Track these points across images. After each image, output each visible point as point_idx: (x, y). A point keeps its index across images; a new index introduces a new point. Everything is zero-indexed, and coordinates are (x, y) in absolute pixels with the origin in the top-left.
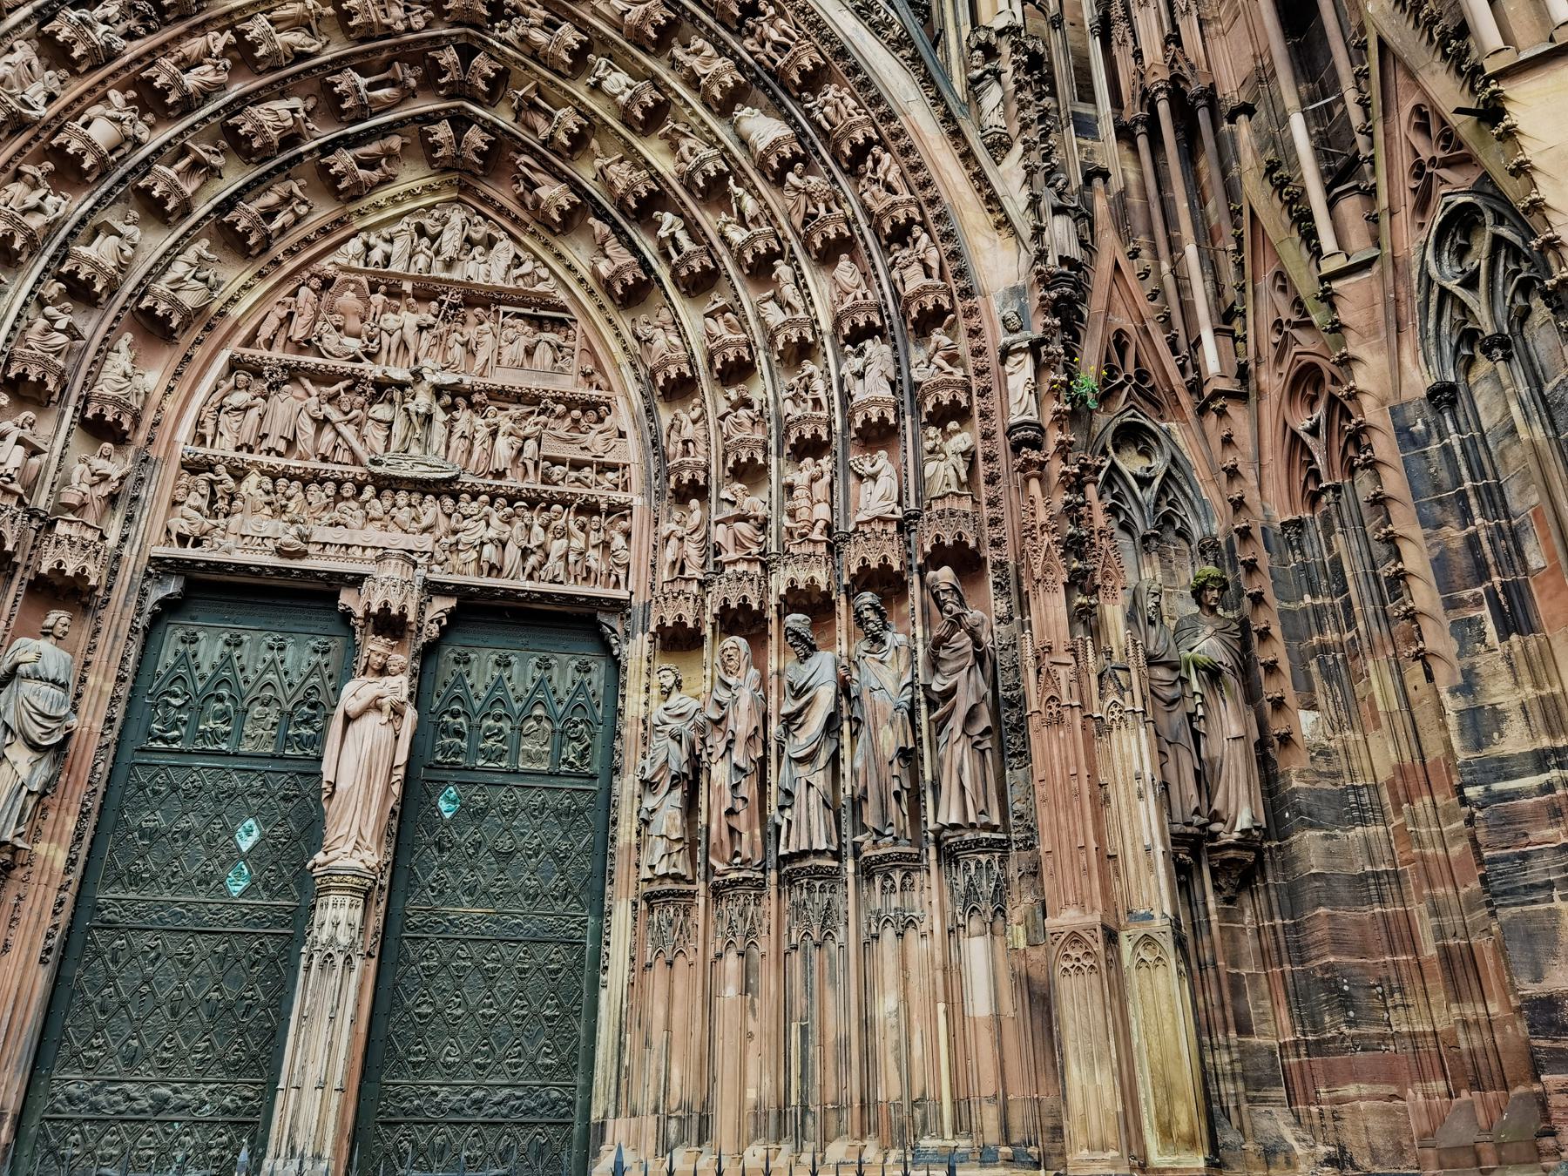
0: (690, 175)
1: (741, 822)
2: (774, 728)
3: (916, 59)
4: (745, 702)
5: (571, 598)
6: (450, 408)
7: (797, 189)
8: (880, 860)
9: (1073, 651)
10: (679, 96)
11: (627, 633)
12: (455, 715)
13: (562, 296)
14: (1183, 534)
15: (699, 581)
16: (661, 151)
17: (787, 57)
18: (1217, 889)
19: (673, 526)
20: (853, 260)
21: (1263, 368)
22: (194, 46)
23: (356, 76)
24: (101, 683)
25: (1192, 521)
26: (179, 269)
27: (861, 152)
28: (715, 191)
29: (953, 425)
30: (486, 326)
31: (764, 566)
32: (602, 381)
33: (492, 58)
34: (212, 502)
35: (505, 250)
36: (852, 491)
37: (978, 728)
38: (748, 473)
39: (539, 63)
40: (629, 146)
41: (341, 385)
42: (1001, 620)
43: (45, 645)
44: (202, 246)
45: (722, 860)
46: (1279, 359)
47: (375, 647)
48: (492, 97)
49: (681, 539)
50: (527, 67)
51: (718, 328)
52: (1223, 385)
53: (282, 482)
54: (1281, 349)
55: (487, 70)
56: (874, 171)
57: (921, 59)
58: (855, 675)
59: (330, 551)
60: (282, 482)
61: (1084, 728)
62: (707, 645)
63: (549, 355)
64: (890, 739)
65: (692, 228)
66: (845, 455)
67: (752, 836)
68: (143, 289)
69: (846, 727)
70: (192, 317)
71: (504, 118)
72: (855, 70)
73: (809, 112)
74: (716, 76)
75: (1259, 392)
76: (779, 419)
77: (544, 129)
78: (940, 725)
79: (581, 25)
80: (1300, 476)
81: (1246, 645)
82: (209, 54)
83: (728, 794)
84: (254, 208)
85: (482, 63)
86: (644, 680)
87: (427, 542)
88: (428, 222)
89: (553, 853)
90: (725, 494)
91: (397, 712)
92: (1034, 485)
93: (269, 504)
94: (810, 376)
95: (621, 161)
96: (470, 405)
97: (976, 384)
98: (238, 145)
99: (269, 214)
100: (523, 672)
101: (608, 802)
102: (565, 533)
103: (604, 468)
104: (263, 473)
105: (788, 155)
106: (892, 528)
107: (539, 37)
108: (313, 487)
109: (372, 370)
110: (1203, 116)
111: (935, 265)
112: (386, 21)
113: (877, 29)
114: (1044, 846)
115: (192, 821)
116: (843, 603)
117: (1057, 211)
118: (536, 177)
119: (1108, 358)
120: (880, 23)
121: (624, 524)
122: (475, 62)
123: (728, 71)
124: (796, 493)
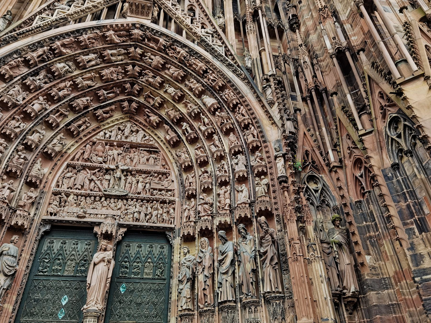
0: (190, 113)
1: (207, 292)
2: (216, 264)
3: (249, 83)
4: (207, 257)
5: (158, 227)
6: (125, 176)
7: (218, 116)
8: (248, 303)
9: (299, 239)
10: (187, 93)
11: (174, 237)
12: (126, 262)
13: (156, 145)
14: (328, 205)
15: (194, 222)
16: (183, 107)
17: (215, 83)
18: (347, 310)
19: (187, 206)
20: (234, 134)
21: (346, 160)
22: (62, 85)
23: (104, 91)
24: (26, 256)
25: (330, 202)
26: (55, 141)
27: (235, 106)
28: (197, 117)
29: (262, 177)
30: (136, 153)
31: (212, 217)
32: (167, 167)
33: (139, 85)
34: (60, 203)
35: (141, 133)
36: (236, 195)
37: (274, 263)
38: (207, 191)
39: (151, 86)
40: (174, 106)
41: (97, 170)
42: (279, 231)
43: (11, 245)
44: (61, 135)
45: (202, 304)
46: (350, 157)
47: (103, 243)
48: (138, 95)
49: (189, 210)
50: (148, 87)
51: (199, 152)
52: (336, 164)
53: (79, 197)
54: (350, 154)
55: (138, 88)
56: (239, 111)
57: (250, 83)
58: (239, 248)
59: (92, 216)
60: (79, 197)
61: (304, 262)
62: (196, 240)
63: (153, 161)
64: (249, 267)
65: (191, 127)
66: (234, 185)
67: (210, 296)
68: (45, 147)
69: (236, 263)
70: (57, 154)
71: (142, 100)
72: (233, 85)
73: (221, 96)
74: (197, 88)
75: (345, 166)
76: (215, 176)
77: (152, 102)
78: (263, 262)
79: (162, 77)
80: (359, 189)
81: (348, 237)
82: (66, 87)
83: (203, 284)
84: (76, 125)
85: (136, 87)
86: (179, 250)
87: (119, 213)
88: (121, 127)
89: (153, 303)
90: (201, 197)
91: (109, 262)
92: (286, 193)
93: (76, 203)
94: (223, 164)
95: (172, 110)
96: (131, 175)
97: (268, 166)
98: (72, 109)
99: (80, 126)
100: (145, 249)
101: (169, 287)
102: (157, 209)
103: (168, 191)
104: (74, 195)
105: (216, 107)
106: (247, 206)
107: (151, 80)
108: (88, 198)
109: (105, 166)
110: (324, 95)
111: (256, 134)
112: (112, 78)
113: (238, 75)
114: (295, 298)
115: (49, 296)
116: (235, 227)
117: (288, 120)
118: (150, 114)
119: (304, 158)
120: (239, 74)
121: (173, 206)
122: (134, 87)
123: (200, 87)
124: (220, 196)
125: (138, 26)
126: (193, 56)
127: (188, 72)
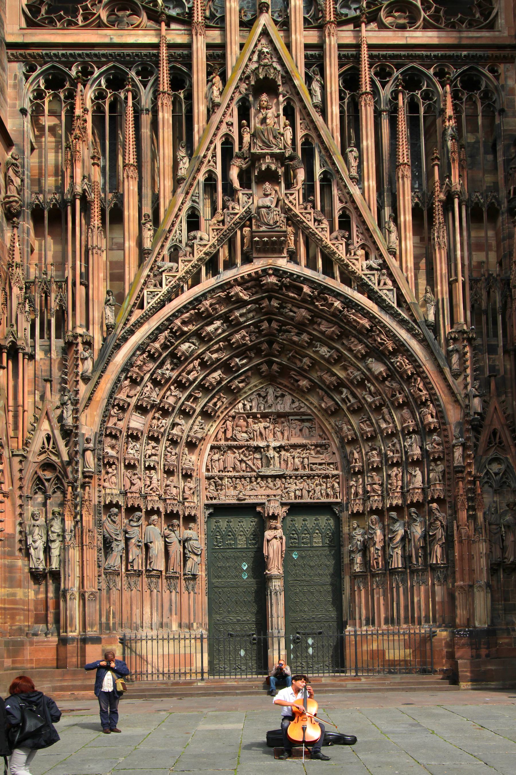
7: (388, 387)
22: (191, 366)
74: (359, 351)
91: (281, 538)
120: (416, 333)
125: (271, 272)
126: (352, 309)
127: (347, 329)
